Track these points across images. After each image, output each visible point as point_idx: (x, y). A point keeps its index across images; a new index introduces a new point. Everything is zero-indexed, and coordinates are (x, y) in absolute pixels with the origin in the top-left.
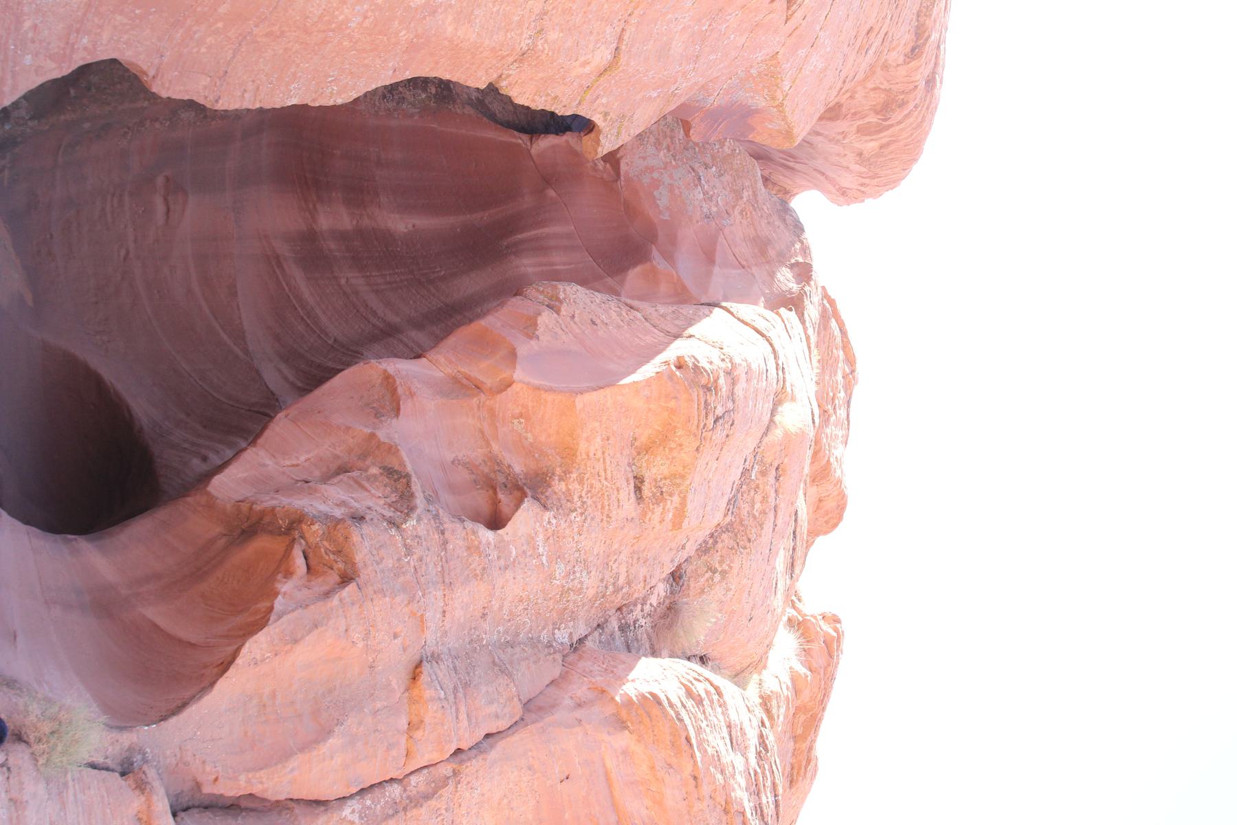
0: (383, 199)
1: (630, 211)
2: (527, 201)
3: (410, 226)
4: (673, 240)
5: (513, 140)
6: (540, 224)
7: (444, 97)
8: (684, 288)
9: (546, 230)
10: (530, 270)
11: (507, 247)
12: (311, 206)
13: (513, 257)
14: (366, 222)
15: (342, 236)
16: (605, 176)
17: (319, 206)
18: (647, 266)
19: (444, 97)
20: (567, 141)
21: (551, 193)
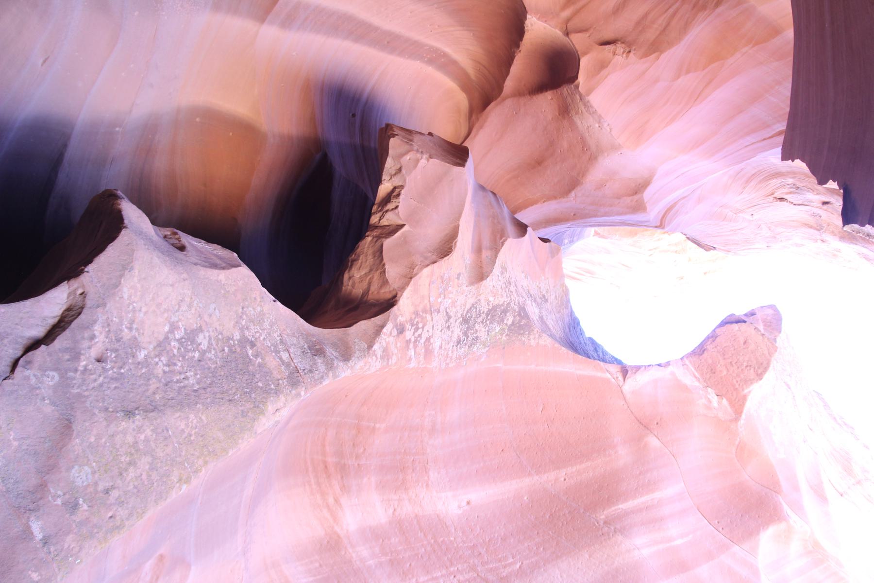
0: (433, 475)
1: (744, 452)
2: (623, 455)
3: (464, 504)
4: (796, 488)
5: (599, 374)
6: (650, 487)
7: (520, 327)
8: (816, 544)
9: (657, 495)
10: (645, 552)
11: (605, 523)
12: (331, 500)
13: (620, 538)
14: (407, 509)
15: (374, 535)
16: (721, 415)
17: (344, 500)
18: (782, 526)
19: (520, 327)
20: (673, 374)
21: (653, 442)
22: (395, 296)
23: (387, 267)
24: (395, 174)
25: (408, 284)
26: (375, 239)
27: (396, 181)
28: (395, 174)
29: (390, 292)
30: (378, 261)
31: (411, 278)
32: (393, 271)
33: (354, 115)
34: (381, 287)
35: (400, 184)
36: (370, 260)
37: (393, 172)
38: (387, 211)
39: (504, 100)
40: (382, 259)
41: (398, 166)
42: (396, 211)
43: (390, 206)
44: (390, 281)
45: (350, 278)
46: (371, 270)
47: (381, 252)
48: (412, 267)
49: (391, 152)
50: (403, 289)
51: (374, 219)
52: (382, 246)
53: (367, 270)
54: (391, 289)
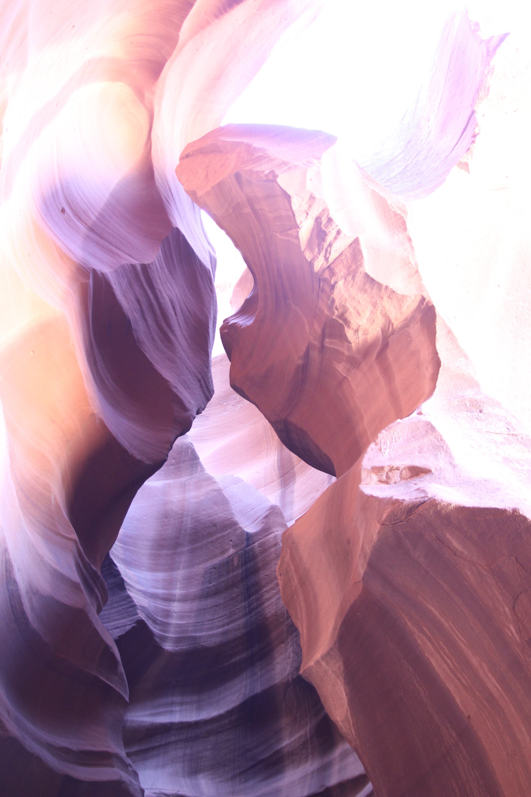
22: (423, 299)
23: (391, 286)
24: (310, 206)
25: (420, 279)
26: (349, 278)
27: (315, 212)
28: (310, 206)
29: (413, 301)
30: (375, 291)
31: (417, 272)
32: (398, 283)
33: (63, 211)
34: (400, 307)
35: (320, 210)
36: (364, 299)
37: (306, 207)
38: (330, 245)
39: (184, 46)
40: (380, 285)
41: (308, 196)
42: (342, 235)
43: (329, 238)
44: (406, 293)
45: (357, 331)
46: (375, 305)
47: (372, 281)
48: (407, 263)
49: (290, 192)
50: (421, 287)
51: (319, 264)
52: (367, 276)
53: (370, 308)
54: (413, 297)
